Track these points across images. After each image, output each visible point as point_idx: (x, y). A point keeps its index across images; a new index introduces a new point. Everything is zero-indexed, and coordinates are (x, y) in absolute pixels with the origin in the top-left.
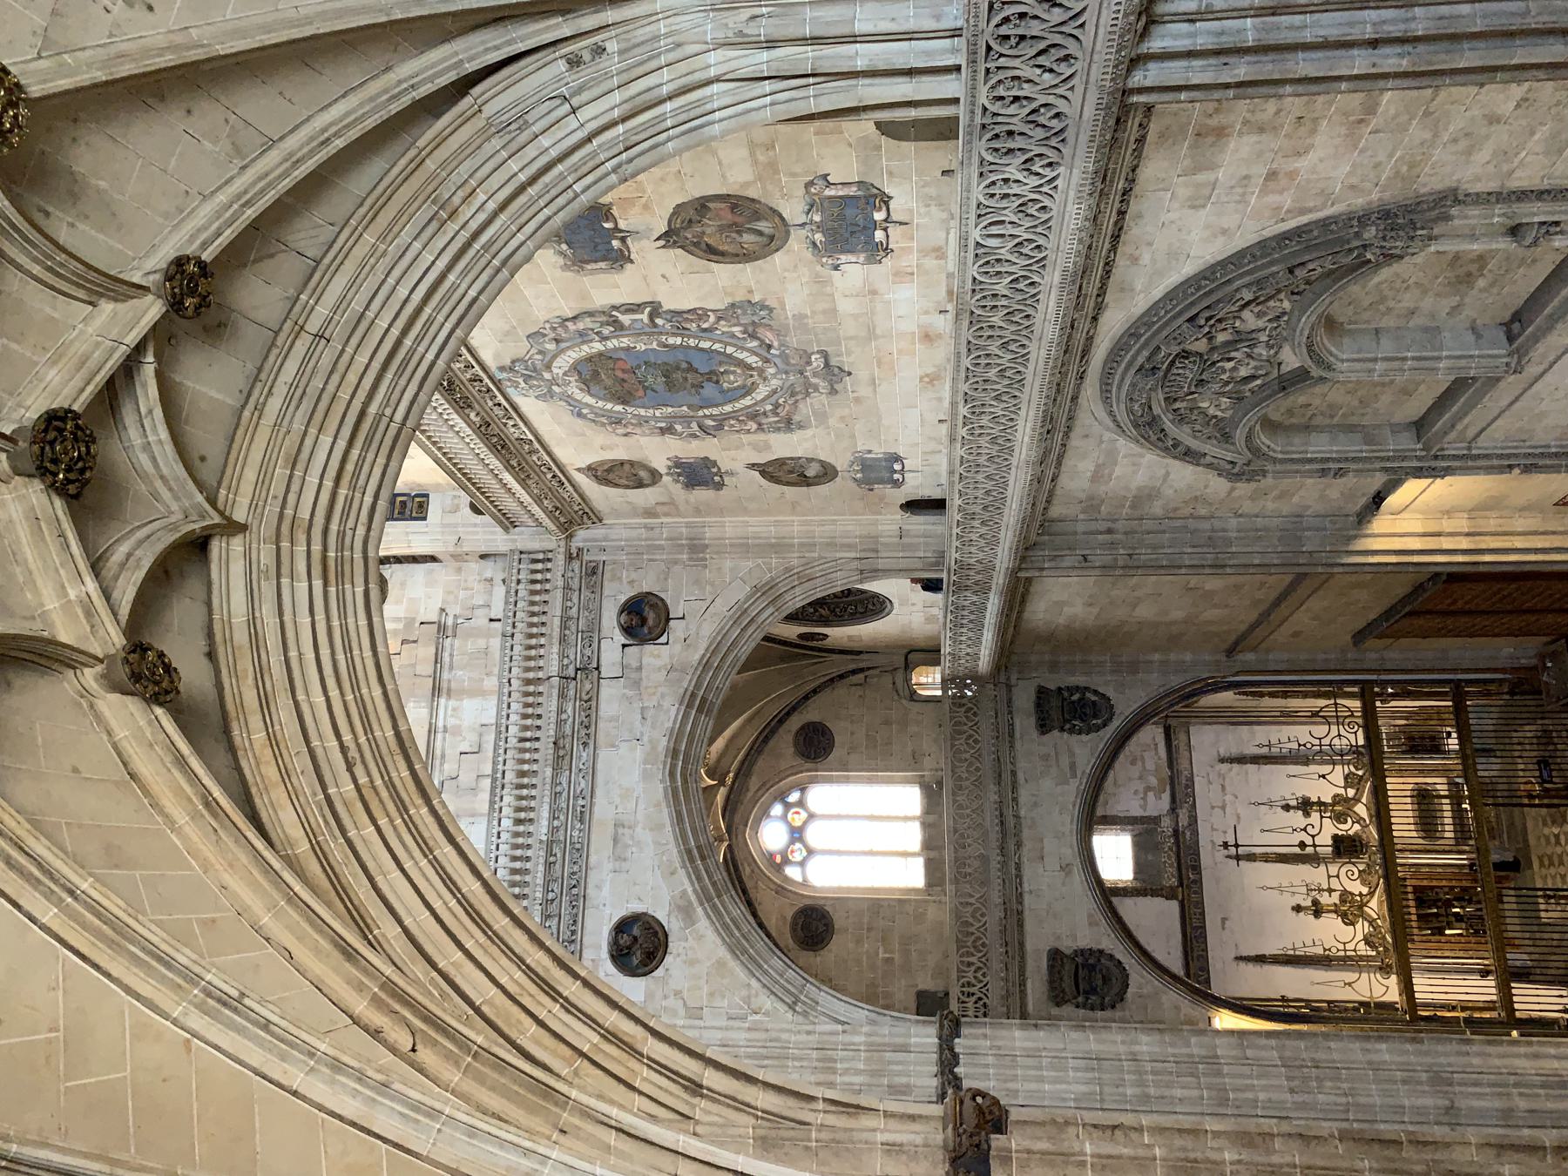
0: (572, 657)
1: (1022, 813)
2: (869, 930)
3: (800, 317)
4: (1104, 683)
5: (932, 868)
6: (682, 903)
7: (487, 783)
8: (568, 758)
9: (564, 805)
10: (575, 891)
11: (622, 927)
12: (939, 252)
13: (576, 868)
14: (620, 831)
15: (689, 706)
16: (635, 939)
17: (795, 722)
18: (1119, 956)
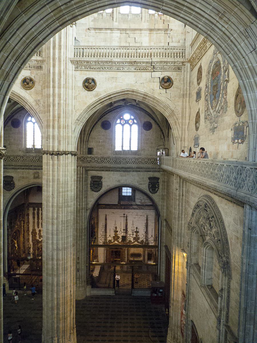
0: (157, 65)
1: (131, 173)
2: (106, 138)
3: (223, 120)
4: (160, 192)
5: (119, 152)
6: (99, 94)
7: (128, 45)
8: (132, 65)
9: (121, 65)
10: (101, 68)
11: (93, 80)
12: (232, 156)
13: (106, 68)
14: (115, 79)
15: (144, 95)
16: (90, 84)
17: (152, 122)
18: (101, 190)
